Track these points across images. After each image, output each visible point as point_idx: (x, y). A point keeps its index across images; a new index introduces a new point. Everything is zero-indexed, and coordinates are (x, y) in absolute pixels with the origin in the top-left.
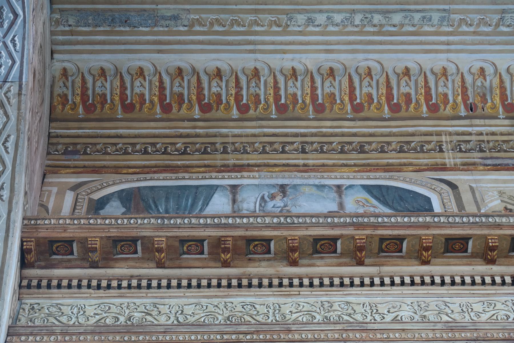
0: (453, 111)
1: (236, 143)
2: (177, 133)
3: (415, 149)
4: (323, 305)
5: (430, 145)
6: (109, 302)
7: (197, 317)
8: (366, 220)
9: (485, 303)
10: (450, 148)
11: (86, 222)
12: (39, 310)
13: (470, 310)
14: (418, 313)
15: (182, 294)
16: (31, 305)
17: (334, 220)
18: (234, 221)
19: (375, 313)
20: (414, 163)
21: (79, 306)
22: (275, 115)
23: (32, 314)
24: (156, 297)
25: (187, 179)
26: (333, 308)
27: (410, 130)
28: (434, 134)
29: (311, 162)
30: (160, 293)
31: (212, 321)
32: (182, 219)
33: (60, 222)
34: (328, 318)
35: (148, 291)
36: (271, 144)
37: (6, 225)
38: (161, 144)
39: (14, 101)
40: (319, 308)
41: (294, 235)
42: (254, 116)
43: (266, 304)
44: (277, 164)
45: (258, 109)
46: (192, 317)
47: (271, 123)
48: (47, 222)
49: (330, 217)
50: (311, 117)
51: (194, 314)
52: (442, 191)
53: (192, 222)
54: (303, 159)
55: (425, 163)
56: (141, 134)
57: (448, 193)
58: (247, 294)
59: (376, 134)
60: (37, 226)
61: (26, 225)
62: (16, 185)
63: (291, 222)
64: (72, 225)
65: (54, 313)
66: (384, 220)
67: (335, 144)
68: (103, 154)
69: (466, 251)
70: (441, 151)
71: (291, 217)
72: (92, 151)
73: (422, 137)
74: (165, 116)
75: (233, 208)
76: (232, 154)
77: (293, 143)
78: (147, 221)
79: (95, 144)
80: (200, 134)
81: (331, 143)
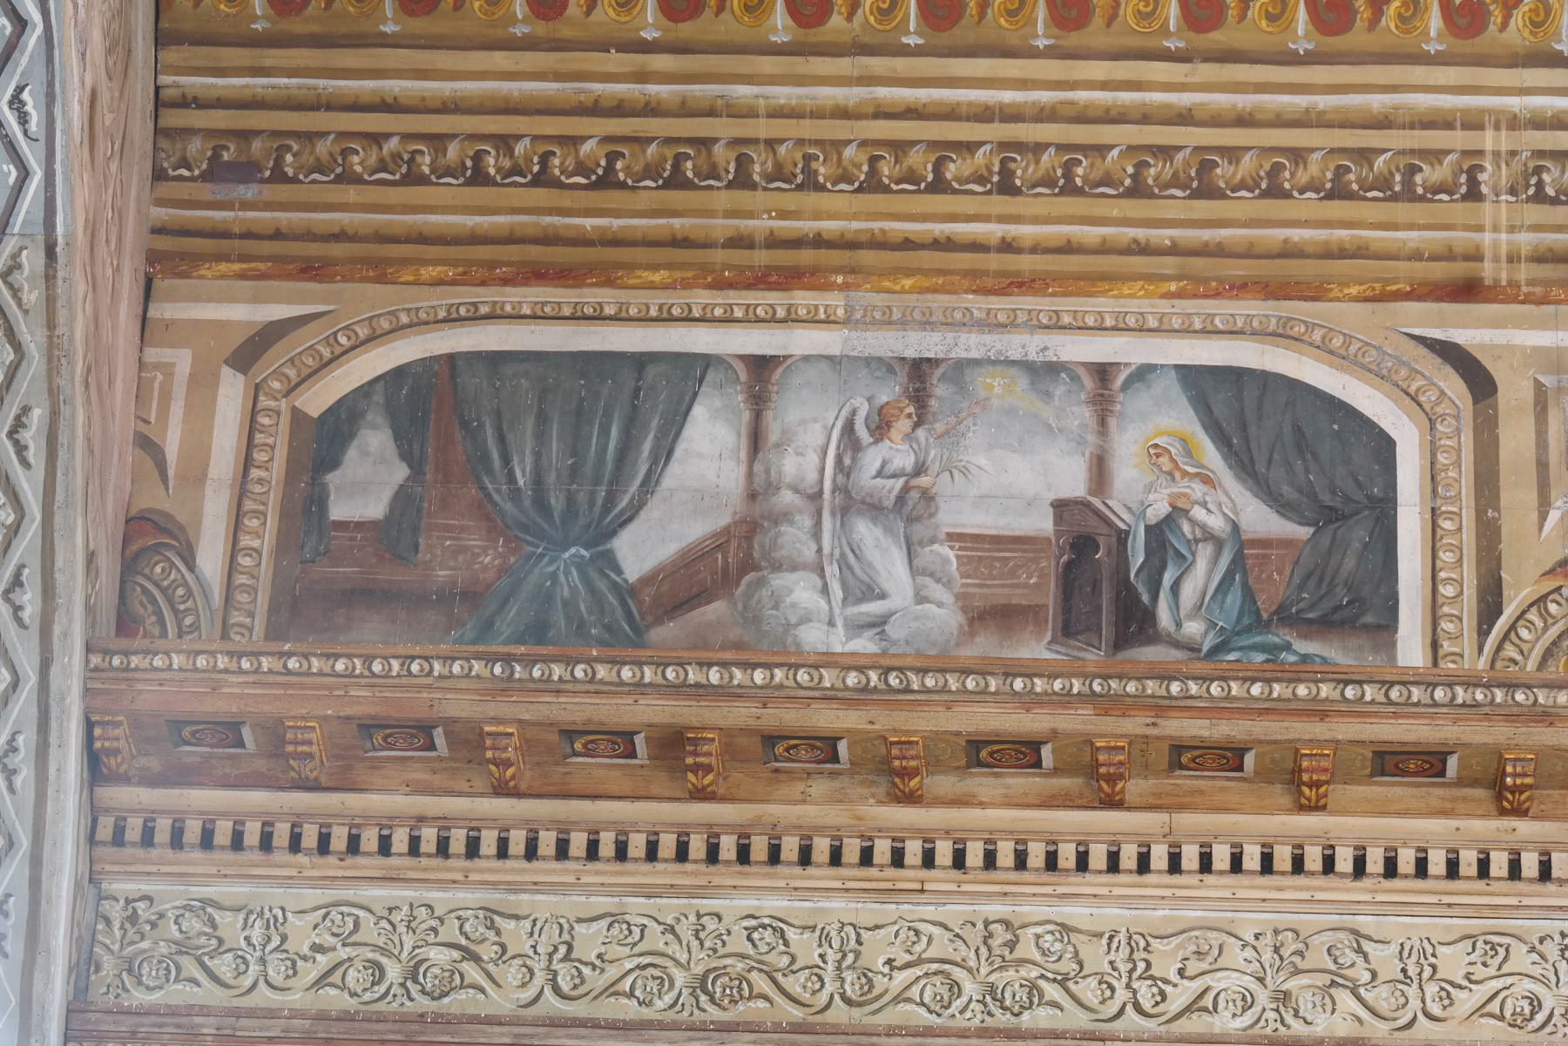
0: (1531, 32)
1: (782, 141)
2: (582, 97)
3: (1384, 183)
4: (991, 935)
5: (1437, 167)
6: (356, 900)
7: (612, 972)
8: (1131, 687)
9: (1480, 944)
10: (1504, 182)
11: (277, 665)
12: (154, 925)
13: (1428, 971)
14: (1268, 980)
15: (571, 879)
16: (128, 901)
17: (1033, 684)
18: (726, 676)
19: (1140, 978)
20: (1374, 247)
21: (267, 914)
22: (915, 33)
23: (132, 943)
24: (494, 885)
25: (610, 318)
26: (1020, 952)
27: (1377, 102)
28: (1458, 124)
29: (1026, 232)
30: (506, 872)
31: (655, 990)
32: (568, 665)
33: (199, 665)
34: (999, 991)
35: (468, 864)
36: (900, 147)
37: (39, 706)
38: (527, 141)
39: (33, 297)
40: (976, 951)
41: (908, 731)
42: (846, 38)
43: (819, 927)
44: (913, 237)
45: (860, 11)
46: (598, 972)
47: (901, 65)
48: (160, 663)
49: (1021, 675)
50: (1041, 43)
51: (603, 961)
52: (1439, 410)
53: (599, 676)
54: (1002, 219)
55: (1411, 244)
56: (461, 99)
57: (1457, 418)
58: (766, 883)
59: (1259, 117)
60: (130, 675)
61: (96, 669)
62: (57, 575)
63: (901, 687)
64: (234, 672)
65: (196, 942)
66: (1187, 690)
67: (1115, 153)
68: (339, 179)
69: (1442, 773)
70: (1474, 194)
71: (900, 669)
72: (302, 167)
73: (1416, 132)
74: (541, 29)
75: (750, 474)
76: (765, 189)
77: (970, 147)
78: (462, 667)
79: (310, 137)
80: (659, 103)
81: (1102, 150)
